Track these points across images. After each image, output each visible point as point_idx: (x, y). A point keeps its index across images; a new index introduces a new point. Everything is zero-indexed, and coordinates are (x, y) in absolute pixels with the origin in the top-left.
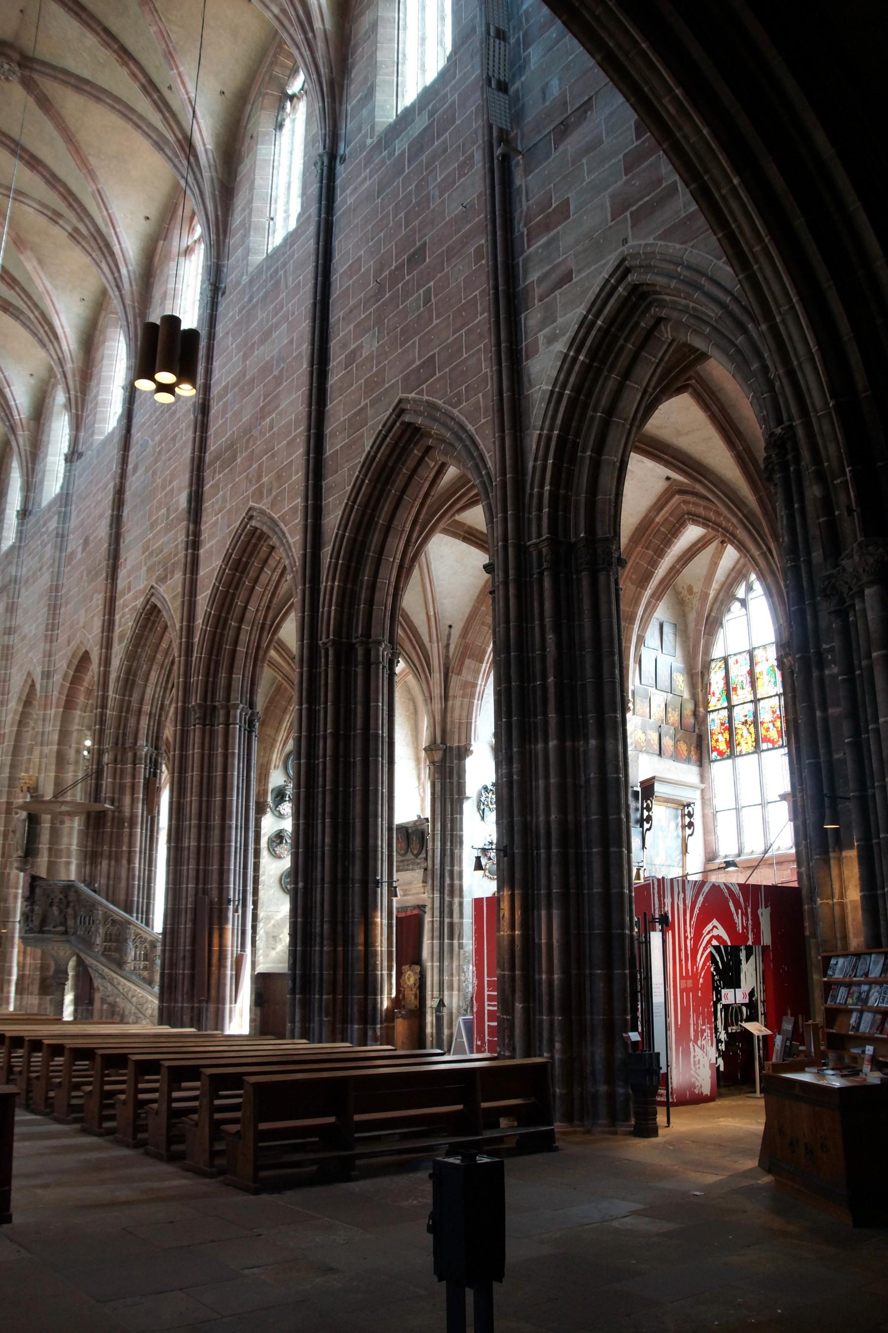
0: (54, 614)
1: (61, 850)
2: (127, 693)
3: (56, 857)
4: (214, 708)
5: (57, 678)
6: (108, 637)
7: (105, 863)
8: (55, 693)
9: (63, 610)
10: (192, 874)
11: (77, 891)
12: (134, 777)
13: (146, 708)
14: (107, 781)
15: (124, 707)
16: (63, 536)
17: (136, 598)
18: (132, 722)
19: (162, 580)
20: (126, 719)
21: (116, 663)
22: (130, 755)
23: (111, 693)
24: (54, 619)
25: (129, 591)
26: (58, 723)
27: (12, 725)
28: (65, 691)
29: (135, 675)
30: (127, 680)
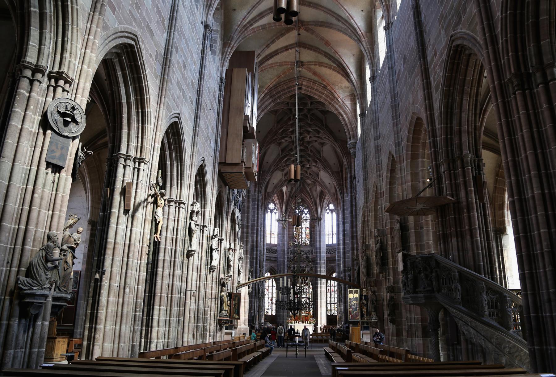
0: (395, 110)
1: (424, 245)
2: (449, 122)
3: (421, 250)
4: (529, 76)
5: (404, 143)
6: (428, 93)
7: (454, 240)
8: (405, 152)
9: (400, 105)
10: (541, 220)
11: (438, 263)
12: (464, 177)
13: (465, 128)
14: (446, 183)
15: (448, 131)
16: (392, 68)
17: (441, 55)
18: (456, 140)
19: (457, 24)
20: (451, 139)
21: (436, 105)
22: (459, 163)
23: (437, 126)
24: (396, 113)
25: (436, 54)
26: (409, 169)
27: (386, 186)
28: (410, 149)
29: (452, 108)
30: (447, 112)
